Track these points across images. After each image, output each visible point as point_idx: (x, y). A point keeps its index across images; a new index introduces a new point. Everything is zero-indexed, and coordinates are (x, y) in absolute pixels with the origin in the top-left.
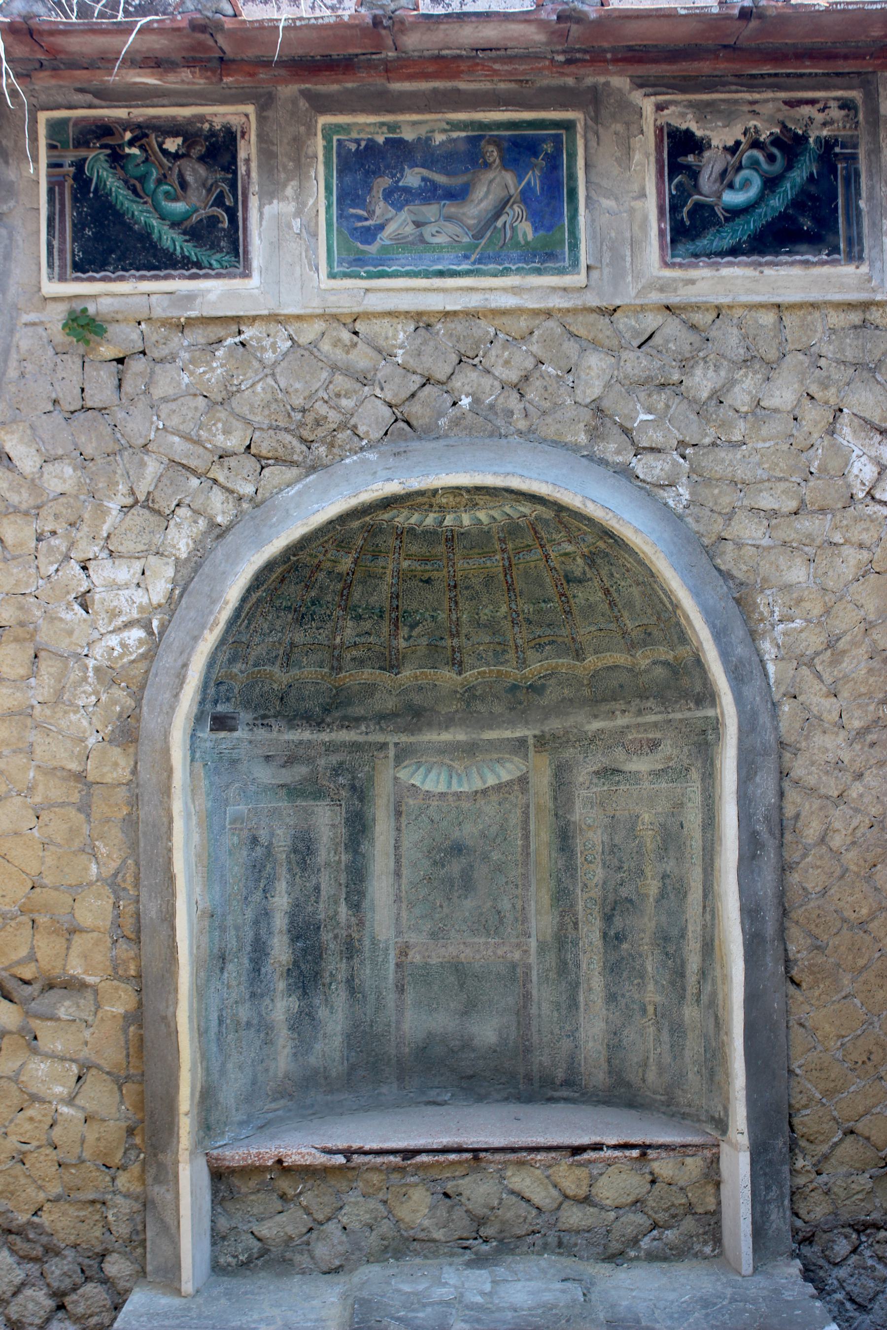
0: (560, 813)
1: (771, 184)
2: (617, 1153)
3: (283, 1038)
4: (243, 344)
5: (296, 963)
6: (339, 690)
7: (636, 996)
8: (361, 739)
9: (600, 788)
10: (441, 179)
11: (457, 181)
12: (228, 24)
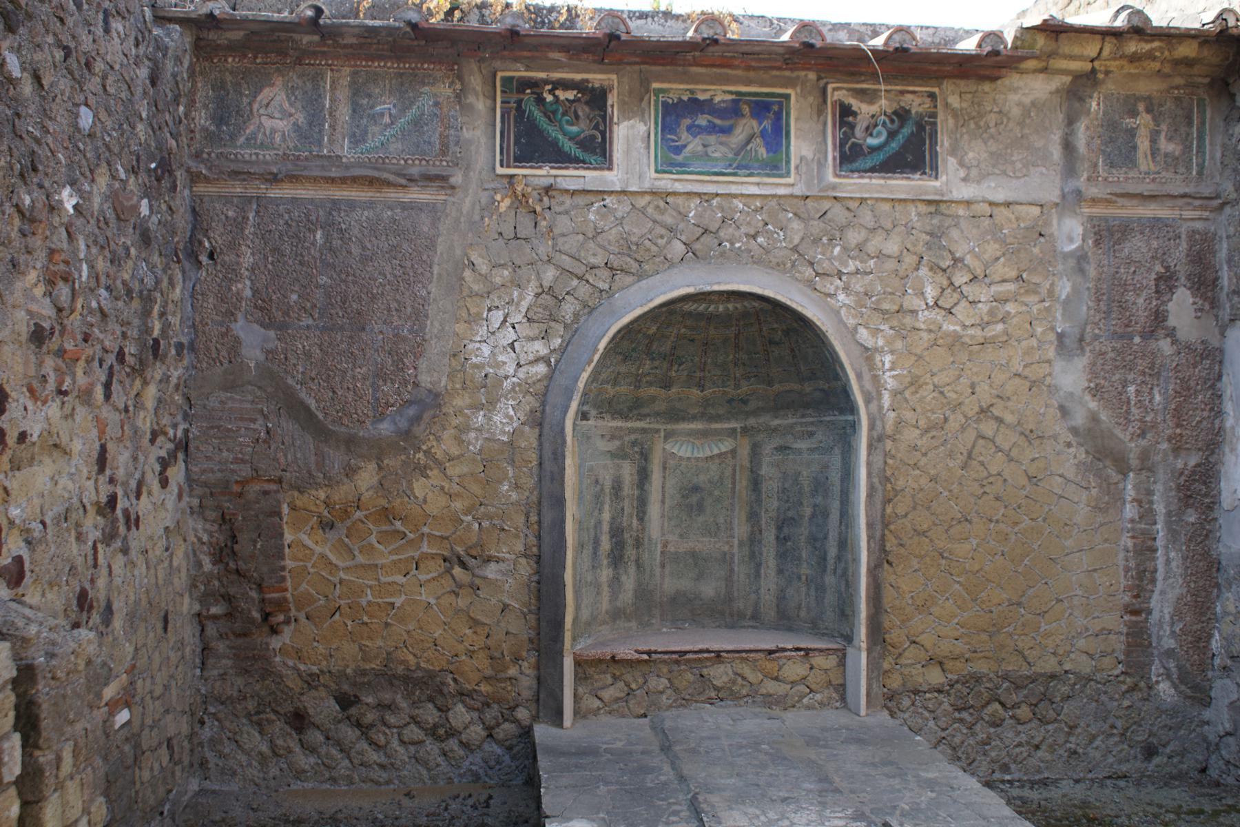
0: (754, 469)
1: (892, 135)
2: (793, 653)
3: (606, 591)
4: (604, 206)
5: (612, 550)
6: (638, 399)
7: (795, 570)
8: (647, 426)
9: (778, 457)
10: (718, 122)
11: (727, 123)
12: (624, 37)
